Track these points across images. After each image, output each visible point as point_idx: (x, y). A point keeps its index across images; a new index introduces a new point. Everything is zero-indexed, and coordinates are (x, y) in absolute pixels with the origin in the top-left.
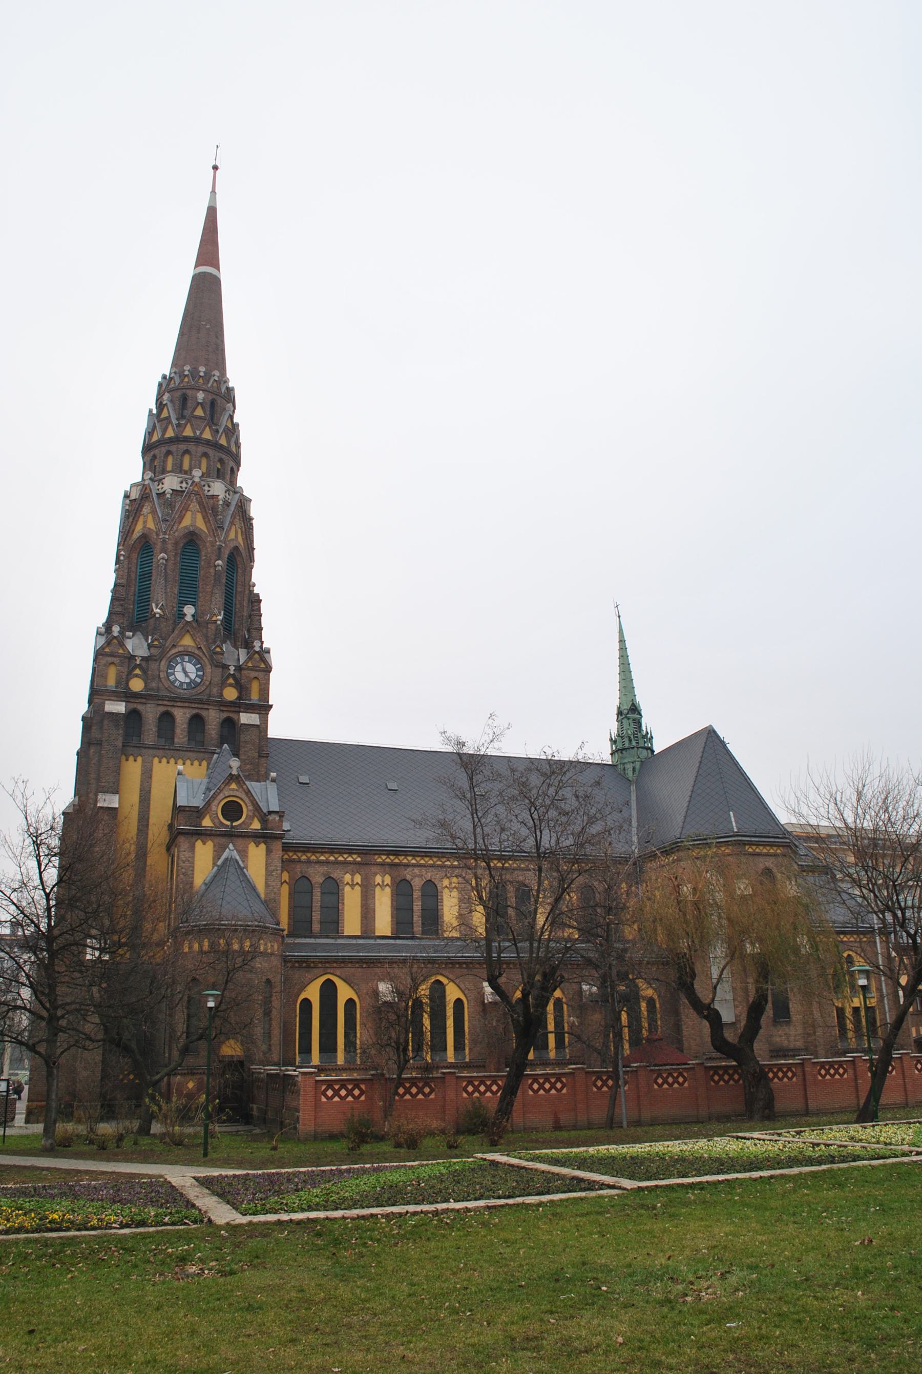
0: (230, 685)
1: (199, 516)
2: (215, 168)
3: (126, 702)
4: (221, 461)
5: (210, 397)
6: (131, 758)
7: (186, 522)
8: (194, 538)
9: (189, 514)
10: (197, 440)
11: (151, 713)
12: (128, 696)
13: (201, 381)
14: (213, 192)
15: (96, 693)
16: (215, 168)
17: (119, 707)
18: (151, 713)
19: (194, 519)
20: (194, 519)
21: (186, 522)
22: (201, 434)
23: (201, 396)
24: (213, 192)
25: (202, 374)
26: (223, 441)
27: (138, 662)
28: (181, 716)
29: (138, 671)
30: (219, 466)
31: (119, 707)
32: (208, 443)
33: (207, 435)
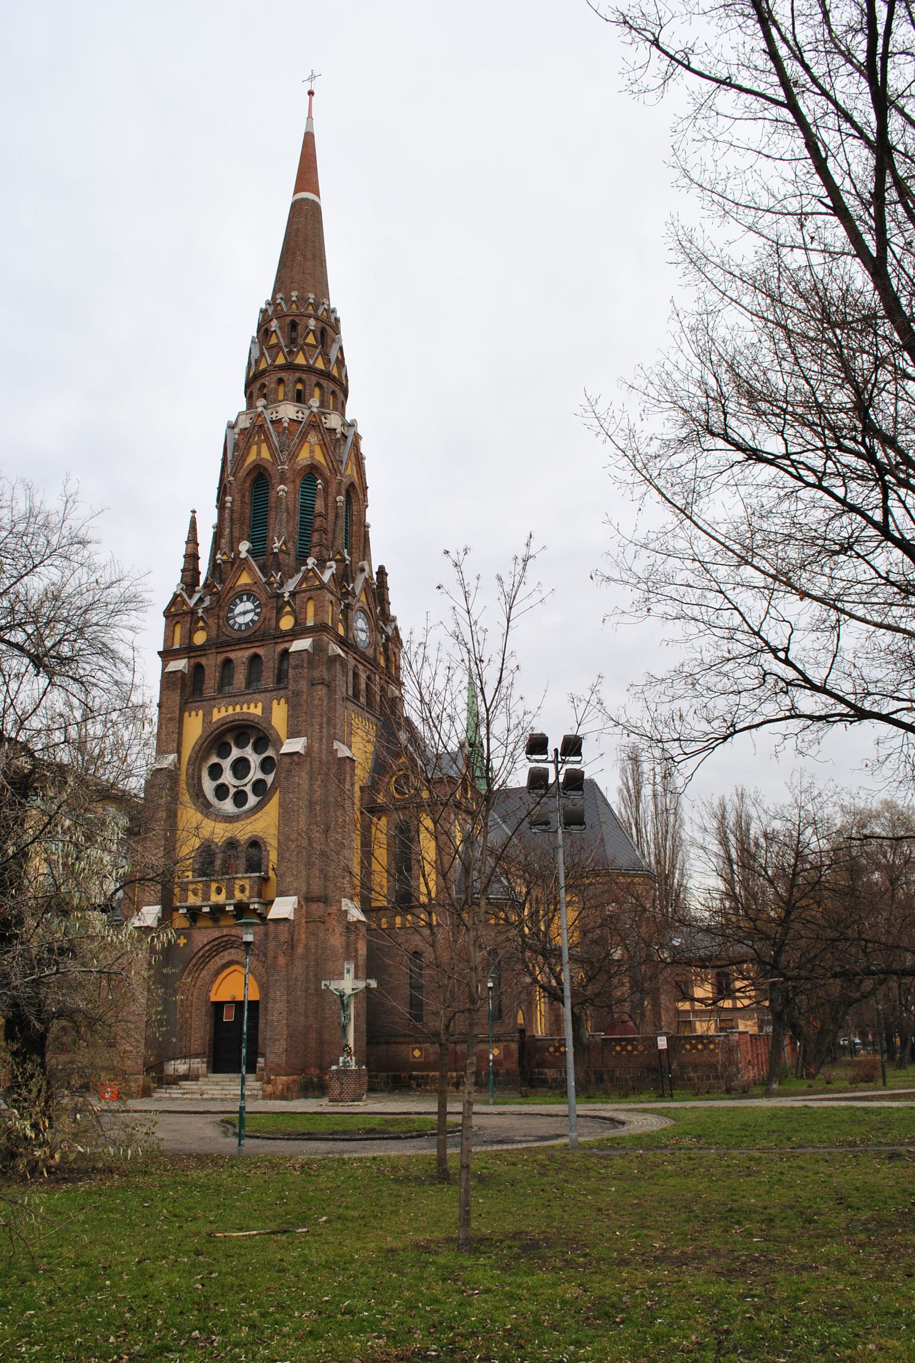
0: (288, 613)
1: (264, 447)
2: (311, 93)
3: (189, 658)
4: (300, 380)
5: (289, 319)
6: (193, 713)
7: (252, 457)
8: (262, 470)
9: (254, 448)
10: (310, 369)
11: (211, 663)
12: (189, 650)
13: (310, 308)
14: (310, 117)
15: (166, 655)
16: (311, 93)
17: (179, 665)
18: (211, 663)
19: (259, 453)
20: (259, 453)
21: (252, 457)
22: (314, 363)
23: (312, 323)
24: (310, 117)
25: (311, 301)
26: (300, 360)
27: (200, 614)
28: (240, 656)
29: (201, 624)
30: (299, 387)
31: (179, 665)
32: (282, 368)
33: (281, 360)
